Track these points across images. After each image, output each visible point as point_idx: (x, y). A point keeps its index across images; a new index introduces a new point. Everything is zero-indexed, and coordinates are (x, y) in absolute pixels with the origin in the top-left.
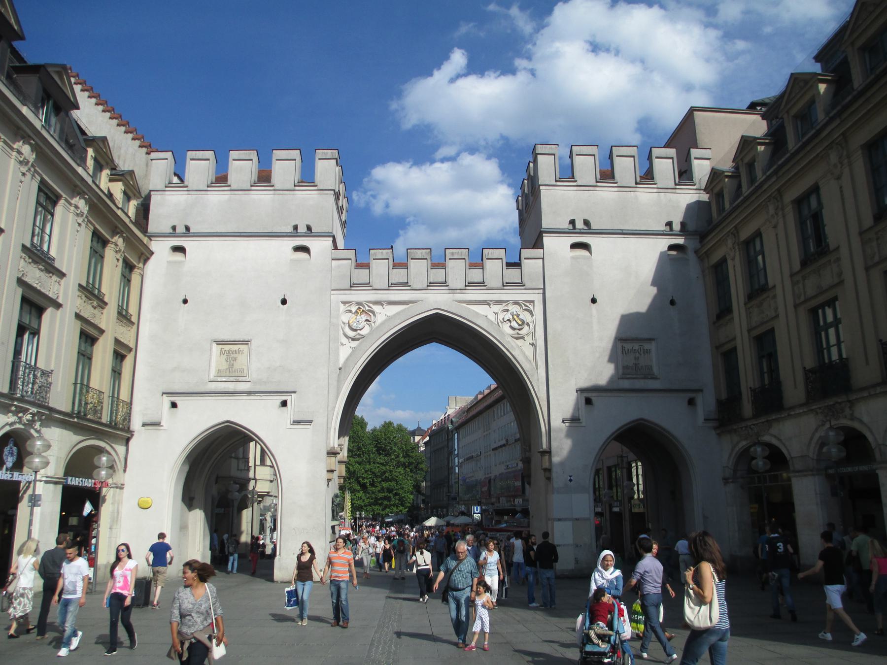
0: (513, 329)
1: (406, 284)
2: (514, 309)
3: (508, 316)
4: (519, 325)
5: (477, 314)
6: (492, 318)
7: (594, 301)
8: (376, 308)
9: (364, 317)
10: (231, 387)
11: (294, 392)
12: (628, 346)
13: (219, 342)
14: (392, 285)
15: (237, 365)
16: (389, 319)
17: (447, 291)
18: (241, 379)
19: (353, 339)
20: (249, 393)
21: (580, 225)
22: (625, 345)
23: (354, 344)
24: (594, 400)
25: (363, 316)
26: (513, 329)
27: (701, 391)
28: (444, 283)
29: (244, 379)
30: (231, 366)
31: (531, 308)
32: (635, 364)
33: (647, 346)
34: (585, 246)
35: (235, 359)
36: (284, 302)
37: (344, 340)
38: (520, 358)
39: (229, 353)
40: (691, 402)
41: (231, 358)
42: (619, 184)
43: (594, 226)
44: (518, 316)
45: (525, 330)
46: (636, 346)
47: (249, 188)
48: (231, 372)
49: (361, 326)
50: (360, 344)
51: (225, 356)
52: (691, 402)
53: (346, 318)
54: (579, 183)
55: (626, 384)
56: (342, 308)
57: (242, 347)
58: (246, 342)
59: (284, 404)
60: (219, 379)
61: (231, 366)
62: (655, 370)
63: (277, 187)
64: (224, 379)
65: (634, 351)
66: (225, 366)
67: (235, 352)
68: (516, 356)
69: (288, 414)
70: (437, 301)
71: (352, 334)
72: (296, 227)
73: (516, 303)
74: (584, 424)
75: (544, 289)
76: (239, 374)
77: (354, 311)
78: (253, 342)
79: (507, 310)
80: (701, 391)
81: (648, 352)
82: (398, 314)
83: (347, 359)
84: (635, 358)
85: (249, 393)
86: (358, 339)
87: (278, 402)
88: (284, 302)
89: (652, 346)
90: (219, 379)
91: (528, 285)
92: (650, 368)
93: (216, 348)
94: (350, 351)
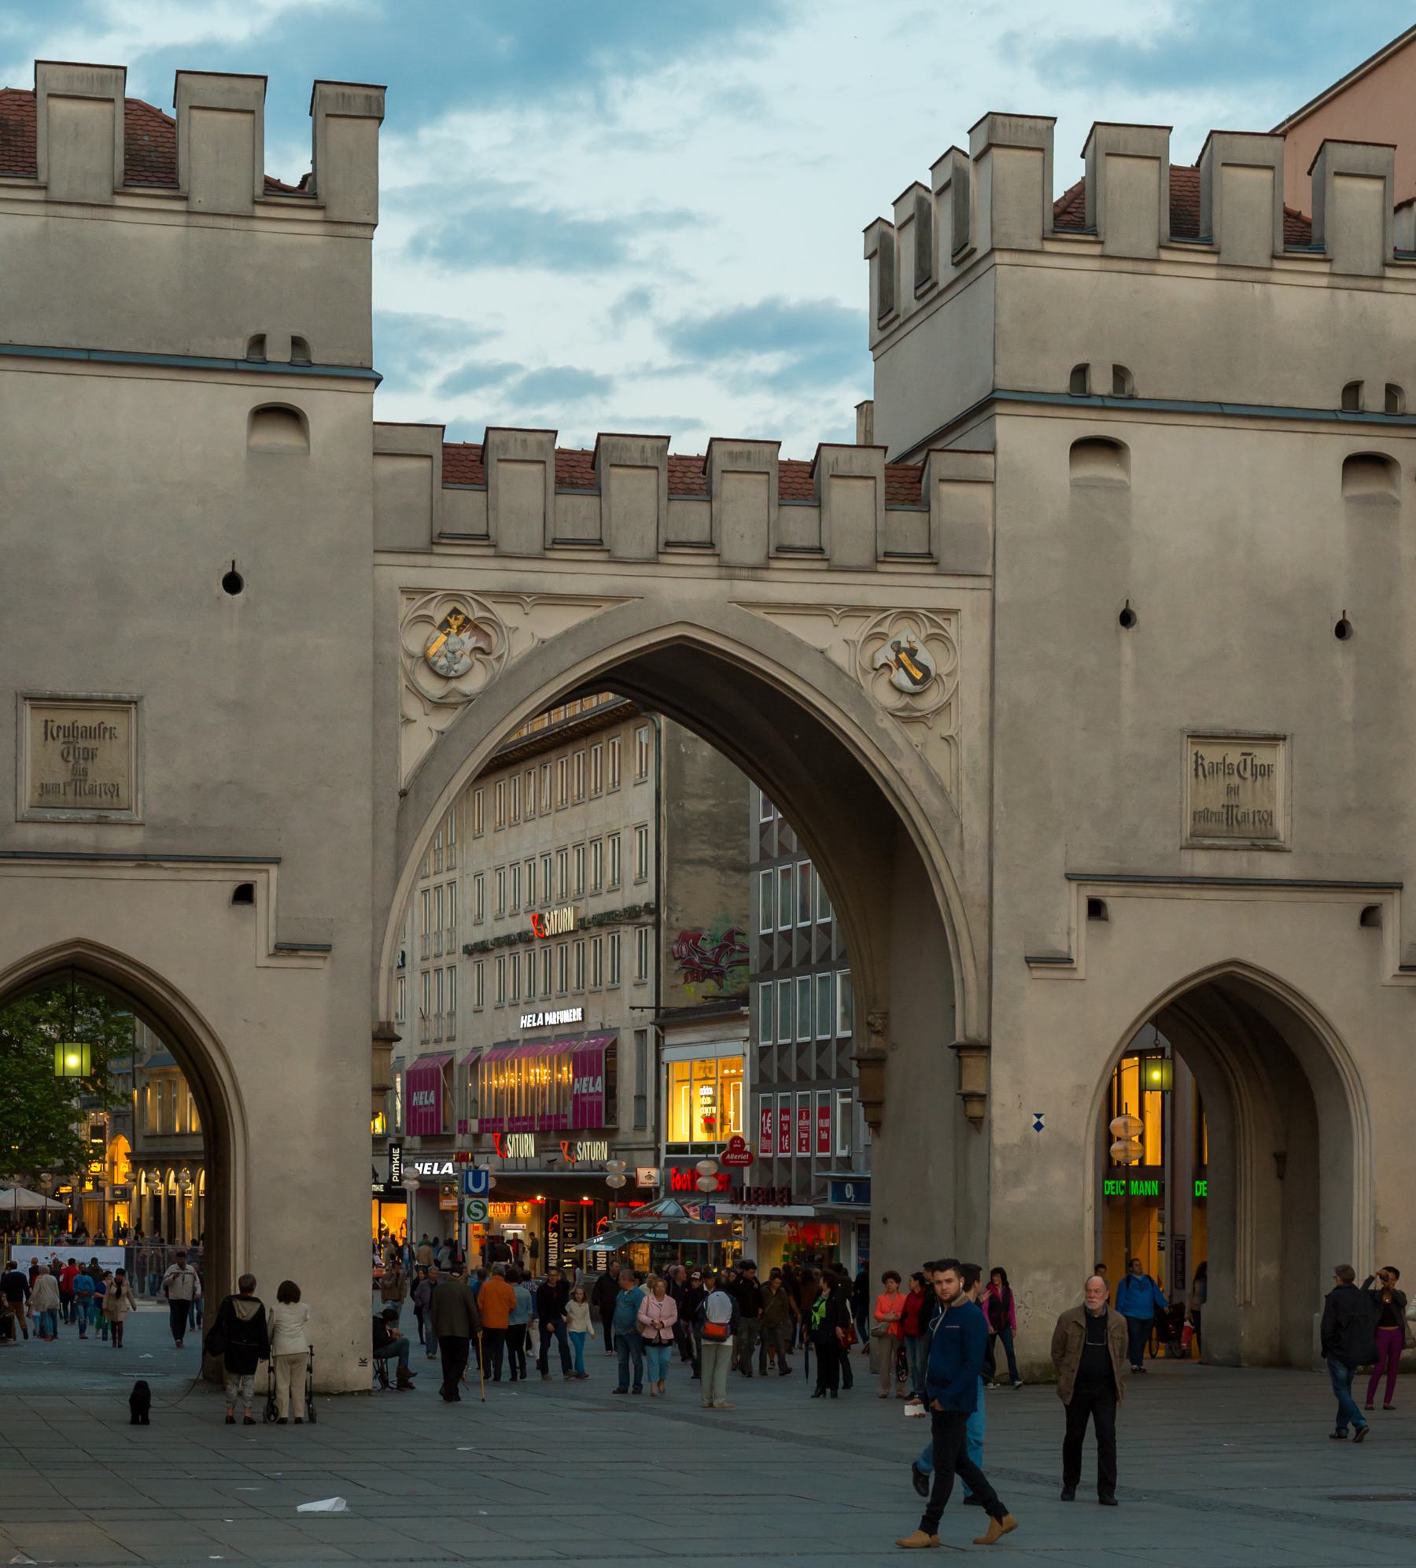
0: (900, 691)
1: (597, 544)
2: (906, 634)
3: (886, 655)
4: (915, 681)
5: (798, 643)
6: (840, 656)
7: (1127, 618)
8: (507, 614)
9: (468, 640)
10: (84, 838)
11: (277, 861)
12: (1212, 754)
13: (39, 701)
14: (555, 545)
15: (98, 773)
16: (545, 648)
17: (714, 572)
18: (114, 815)
19: (439, 705)
20: (143, 860)
21: (1101, 383)
22: (1203, 751)
23: (443, 721)
24: (1113, 906)
25: (465, 635)
26: (900, 691)
27: (1399, 887)
28: (708, 546)
29: (123, 816)
30: (79, 776)
31: (952, 630)
32: (1229, 808)
33: (1263, 755)
34: (1110, 447)
35: (90, 755)
36: (233, 583)
37: (413, 708)
38: (917, 779)
39: (71, 733)
40: (1369, 917)
41: (78, 747)
42: (1225, 258)
43: (1142, 386)
44: (912, 653)
45: (931, 699)
46: (1234, 756)
47: (106, 198)
48: (81, 790)
49: (460, 667)
50: (461, 721)
51: (58, 746)
52: (1369, 917)
53: (413, 641)
54: (1110, 249)
55: (1201, 864)
56: (406, 609)
57: (111, 719)
58: (124, 705)
59: (244, 894)
60: (49, 814)
61: (79, 776)
62: (1281, 825)
63: (200, 201)
64: (64, 815)
65: (1228, 769)
66: (60, 774)
67: (89, 733)
68: (905, 774)
69: (261, 924)
70: (686, 599)
71: (434, 688)
72: (258, 342)
73: (908, 614)
74: (1080, 974)
75: (993, 577)
76: (105, 800)
77: (439, 618)
78: (145, 705)
79: (882, 636)
80: (1399, 887)
81: (1266, 771)
82: (569, 634)
83: (424, 766)
84: (1232, 791)
85: (143, 860)
86: (454, 706)
87: (229, 890)
88: (233, 583)
89: (1277, 757)
90: (49, 814)
91: (948, 560)
92: (1268, 818)
93: (31, 723)
94: (429, 742)
